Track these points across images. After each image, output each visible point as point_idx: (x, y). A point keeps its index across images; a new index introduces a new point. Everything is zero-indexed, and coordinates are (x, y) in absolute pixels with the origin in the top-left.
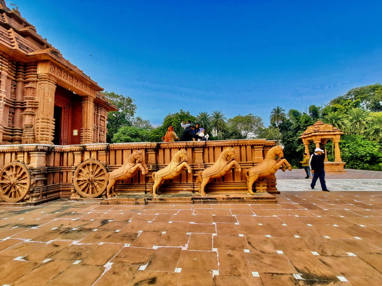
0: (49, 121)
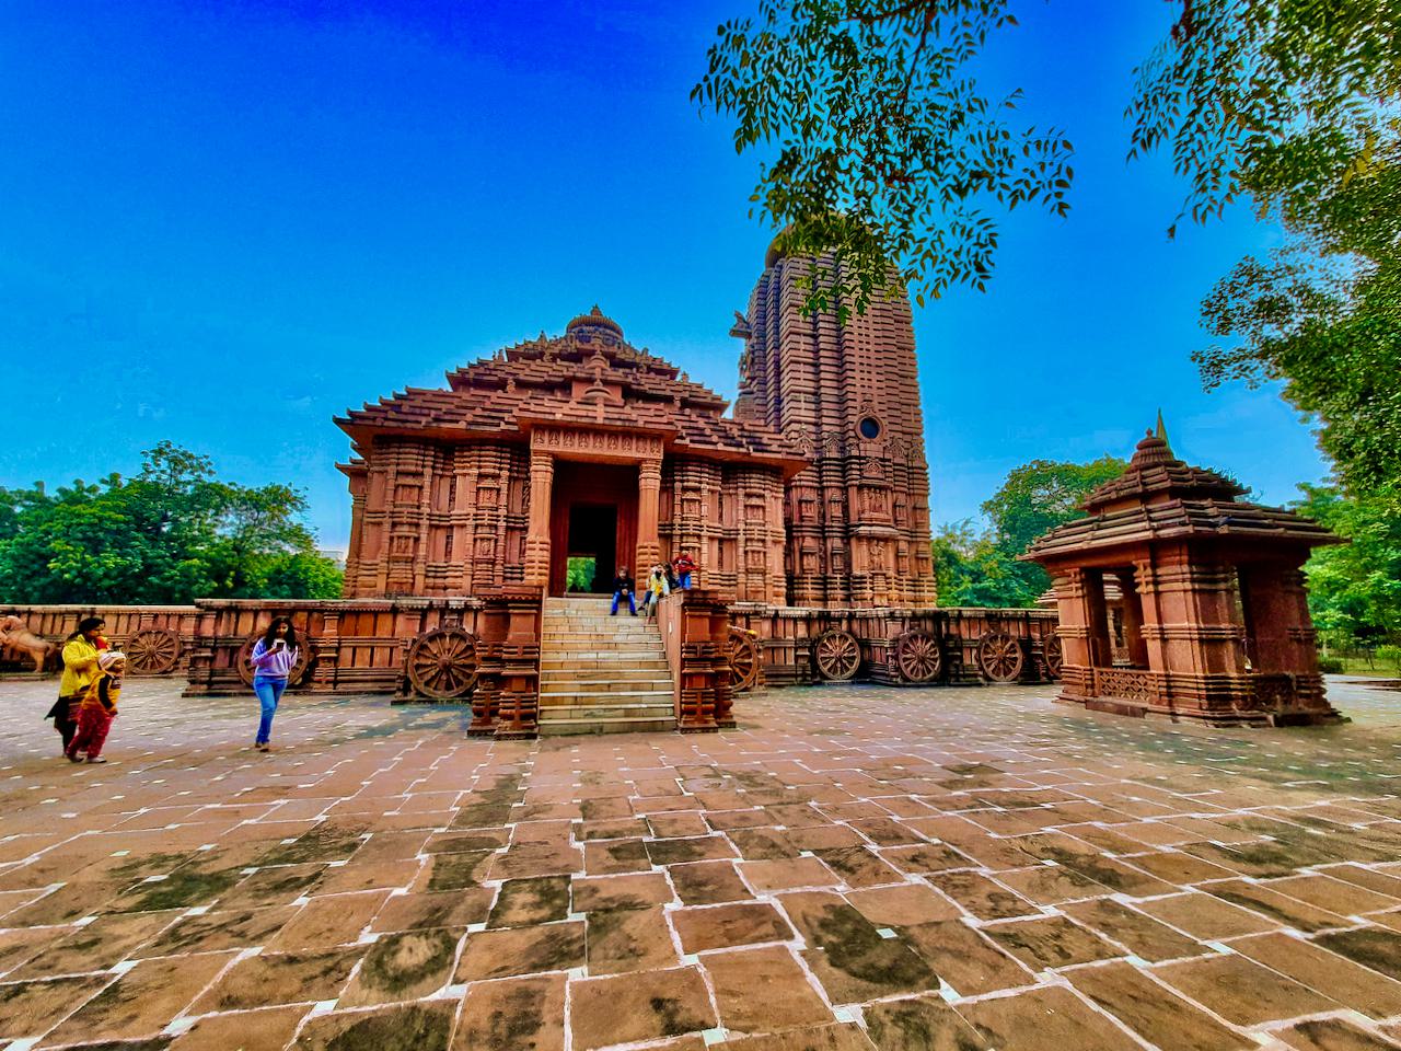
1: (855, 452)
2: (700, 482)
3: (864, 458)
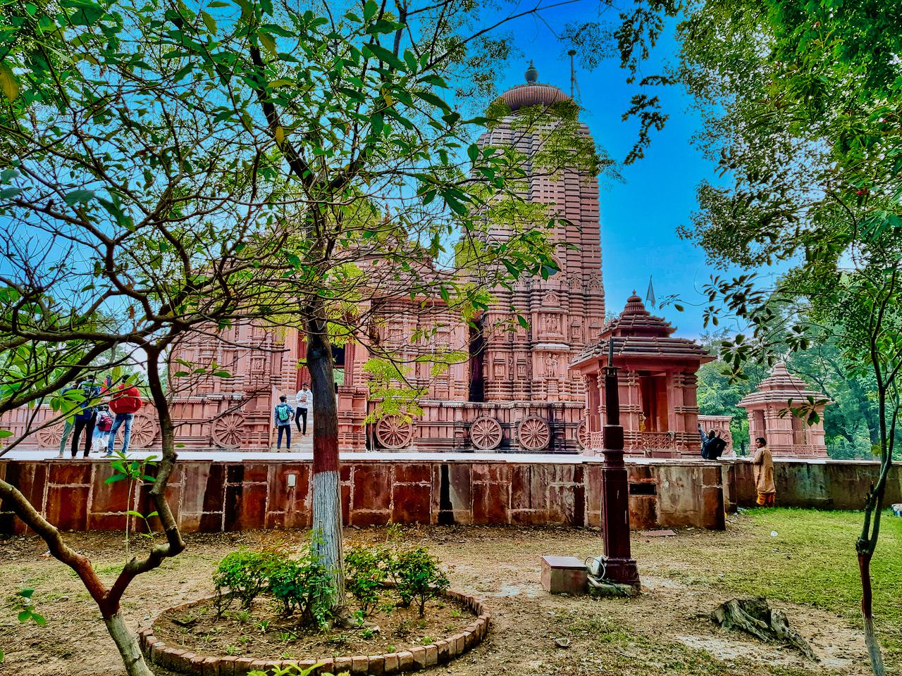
1: (536, 287)
3: (545, 290)
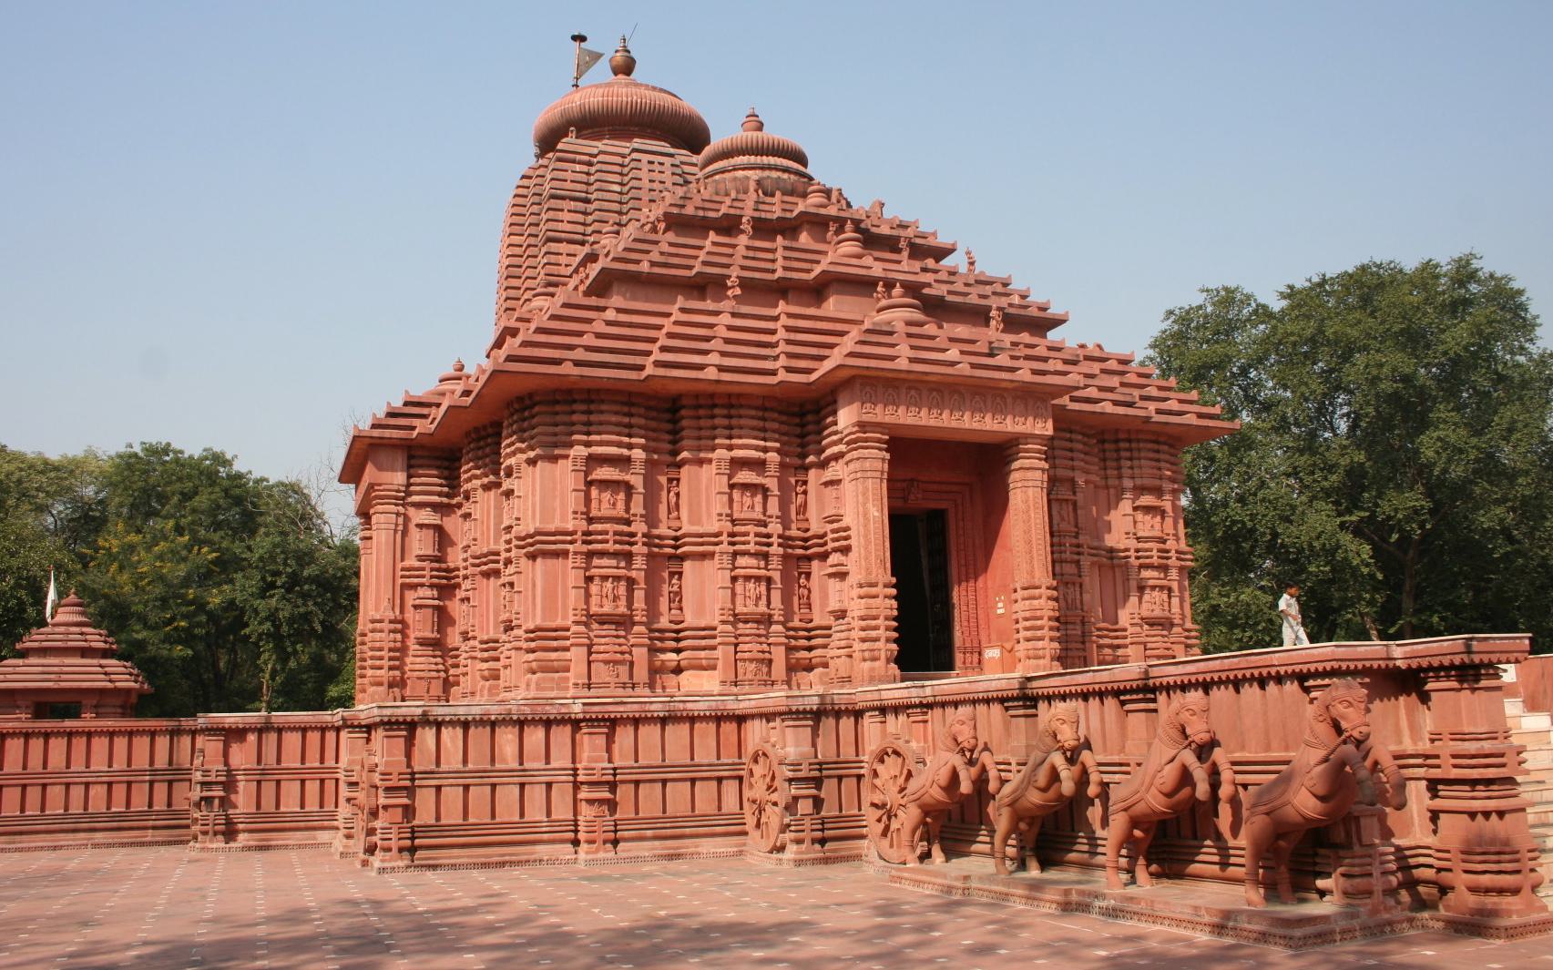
0: (873, 591)
2: (1073, 468)
